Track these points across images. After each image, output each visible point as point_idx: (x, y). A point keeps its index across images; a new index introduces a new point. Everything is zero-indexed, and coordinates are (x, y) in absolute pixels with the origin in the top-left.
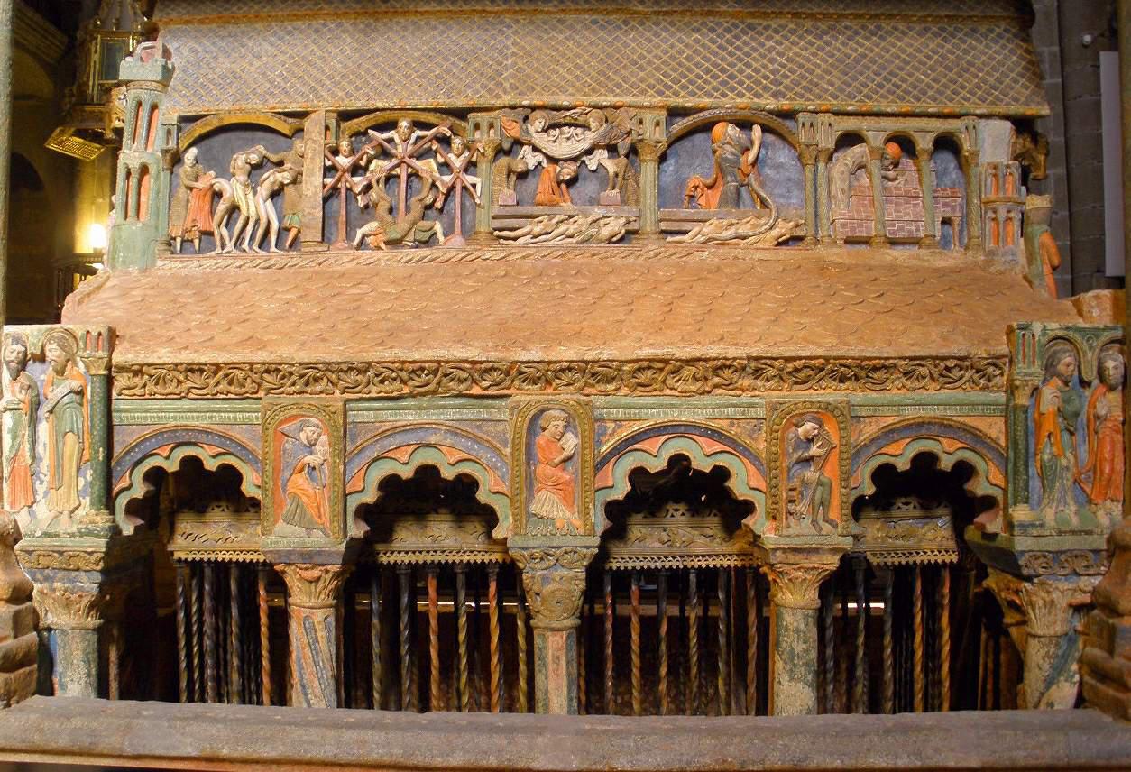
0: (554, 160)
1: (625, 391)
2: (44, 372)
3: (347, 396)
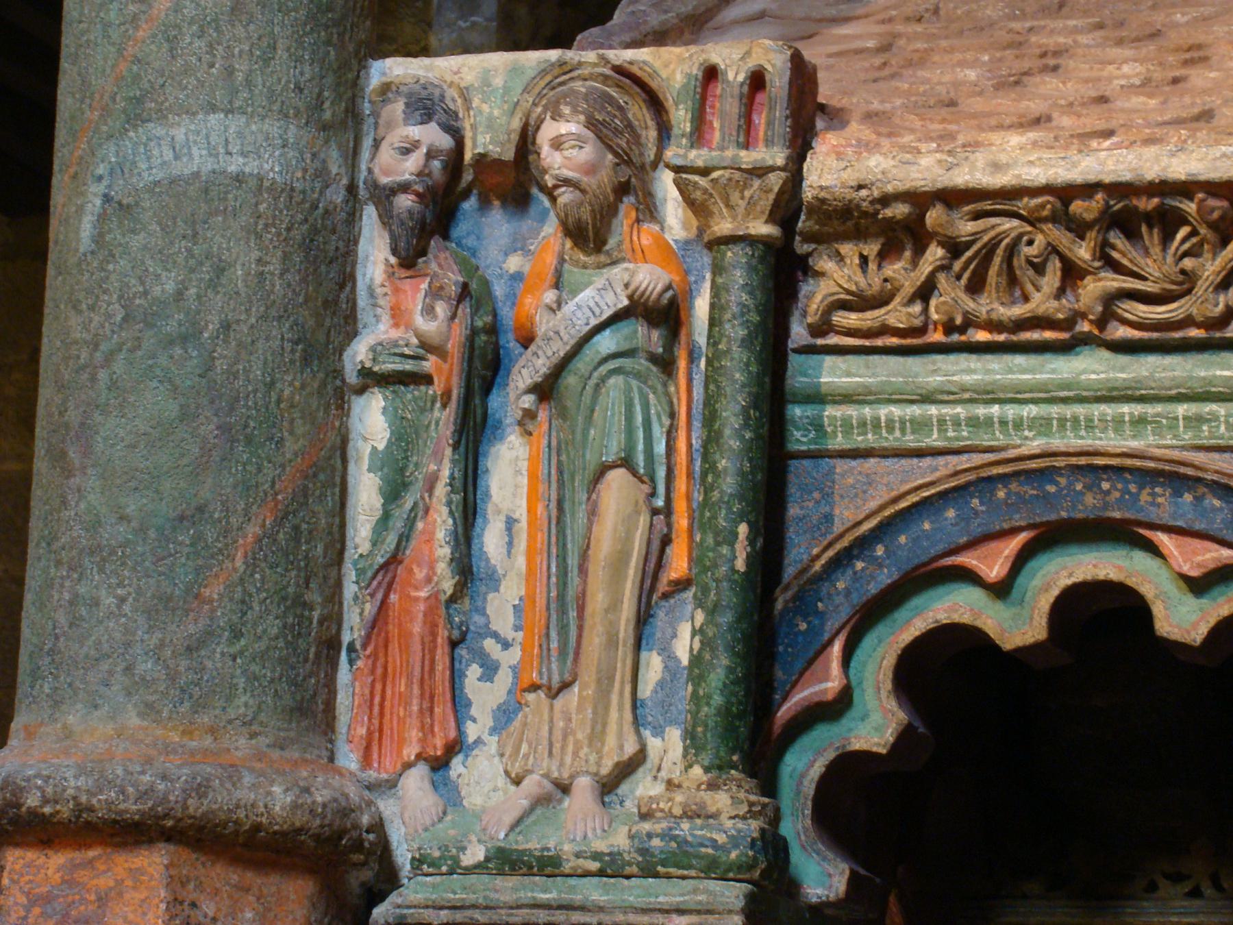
2: (517, 245)
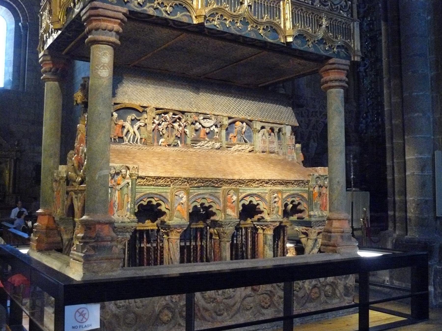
0: (204, 127)
1: (244, 186)
3: (190, 186)
